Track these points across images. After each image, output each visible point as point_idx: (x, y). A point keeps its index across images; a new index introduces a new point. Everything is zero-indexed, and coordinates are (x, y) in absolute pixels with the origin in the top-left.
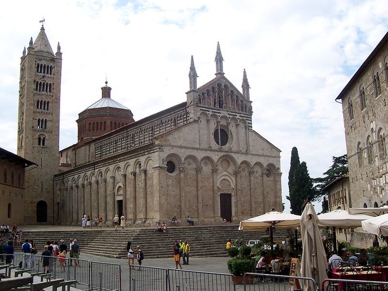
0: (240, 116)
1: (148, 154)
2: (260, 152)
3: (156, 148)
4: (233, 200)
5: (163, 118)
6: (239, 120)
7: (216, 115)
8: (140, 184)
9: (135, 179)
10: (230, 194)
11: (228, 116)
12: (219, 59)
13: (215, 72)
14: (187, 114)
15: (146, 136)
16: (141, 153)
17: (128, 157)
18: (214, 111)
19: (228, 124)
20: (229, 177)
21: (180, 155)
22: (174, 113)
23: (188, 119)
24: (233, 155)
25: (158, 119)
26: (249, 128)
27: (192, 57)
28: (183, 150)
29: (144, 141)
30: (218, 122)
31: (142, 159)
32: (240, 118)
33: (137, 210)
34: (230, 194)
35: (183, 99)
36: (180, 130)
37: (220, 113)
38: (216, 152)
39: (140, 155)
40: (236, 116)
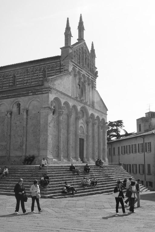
0: (91, 78)
1: (32, 95)
2: (99, 109)
3: (47, 89)
4: (85, 143)
5: (29, 67)
6: (90, 80)
7: (80, 72)
8: (18, 123)
9: (11, 117)
10: (83, 139)
11: (86, 75)
12: (81, 28)
13: (78, 38)
14: (61, 66)
15: (5, 82)
16: (23, 94)
17: (3, 97)
18: (79, 68)
19: (85, 81)
20: (84, 125)
21: (61, 100)
22: (44, 64)
23: (61, 70)
24: (87, 107)
25: (22, 69)
26: (95, 88)
27: (68, 18)
28: (63, 96)
29: (3, 87)
30: (80, 79)
31: (23, 100)
32: (91, 79)
33: (12, 148)
34: (83, 139)
35: (59, 54)
36: (62, 78)
37: (82, 71)
38: (79, 103)
39: (21, 95)
40: (89, 76)
